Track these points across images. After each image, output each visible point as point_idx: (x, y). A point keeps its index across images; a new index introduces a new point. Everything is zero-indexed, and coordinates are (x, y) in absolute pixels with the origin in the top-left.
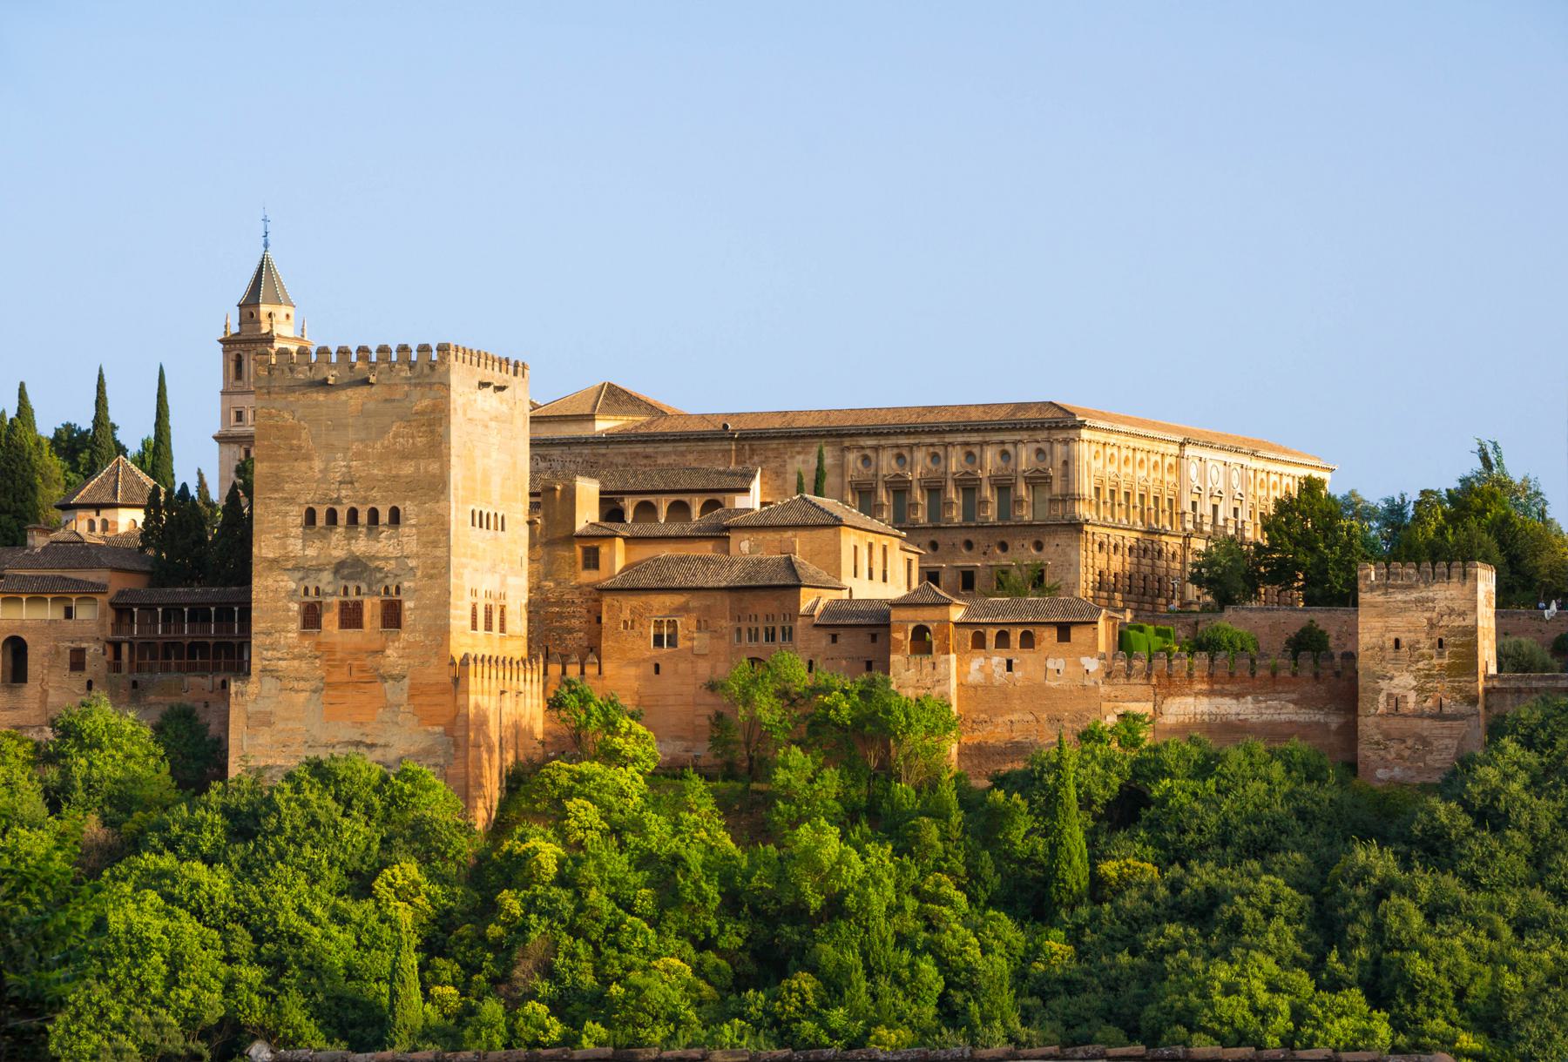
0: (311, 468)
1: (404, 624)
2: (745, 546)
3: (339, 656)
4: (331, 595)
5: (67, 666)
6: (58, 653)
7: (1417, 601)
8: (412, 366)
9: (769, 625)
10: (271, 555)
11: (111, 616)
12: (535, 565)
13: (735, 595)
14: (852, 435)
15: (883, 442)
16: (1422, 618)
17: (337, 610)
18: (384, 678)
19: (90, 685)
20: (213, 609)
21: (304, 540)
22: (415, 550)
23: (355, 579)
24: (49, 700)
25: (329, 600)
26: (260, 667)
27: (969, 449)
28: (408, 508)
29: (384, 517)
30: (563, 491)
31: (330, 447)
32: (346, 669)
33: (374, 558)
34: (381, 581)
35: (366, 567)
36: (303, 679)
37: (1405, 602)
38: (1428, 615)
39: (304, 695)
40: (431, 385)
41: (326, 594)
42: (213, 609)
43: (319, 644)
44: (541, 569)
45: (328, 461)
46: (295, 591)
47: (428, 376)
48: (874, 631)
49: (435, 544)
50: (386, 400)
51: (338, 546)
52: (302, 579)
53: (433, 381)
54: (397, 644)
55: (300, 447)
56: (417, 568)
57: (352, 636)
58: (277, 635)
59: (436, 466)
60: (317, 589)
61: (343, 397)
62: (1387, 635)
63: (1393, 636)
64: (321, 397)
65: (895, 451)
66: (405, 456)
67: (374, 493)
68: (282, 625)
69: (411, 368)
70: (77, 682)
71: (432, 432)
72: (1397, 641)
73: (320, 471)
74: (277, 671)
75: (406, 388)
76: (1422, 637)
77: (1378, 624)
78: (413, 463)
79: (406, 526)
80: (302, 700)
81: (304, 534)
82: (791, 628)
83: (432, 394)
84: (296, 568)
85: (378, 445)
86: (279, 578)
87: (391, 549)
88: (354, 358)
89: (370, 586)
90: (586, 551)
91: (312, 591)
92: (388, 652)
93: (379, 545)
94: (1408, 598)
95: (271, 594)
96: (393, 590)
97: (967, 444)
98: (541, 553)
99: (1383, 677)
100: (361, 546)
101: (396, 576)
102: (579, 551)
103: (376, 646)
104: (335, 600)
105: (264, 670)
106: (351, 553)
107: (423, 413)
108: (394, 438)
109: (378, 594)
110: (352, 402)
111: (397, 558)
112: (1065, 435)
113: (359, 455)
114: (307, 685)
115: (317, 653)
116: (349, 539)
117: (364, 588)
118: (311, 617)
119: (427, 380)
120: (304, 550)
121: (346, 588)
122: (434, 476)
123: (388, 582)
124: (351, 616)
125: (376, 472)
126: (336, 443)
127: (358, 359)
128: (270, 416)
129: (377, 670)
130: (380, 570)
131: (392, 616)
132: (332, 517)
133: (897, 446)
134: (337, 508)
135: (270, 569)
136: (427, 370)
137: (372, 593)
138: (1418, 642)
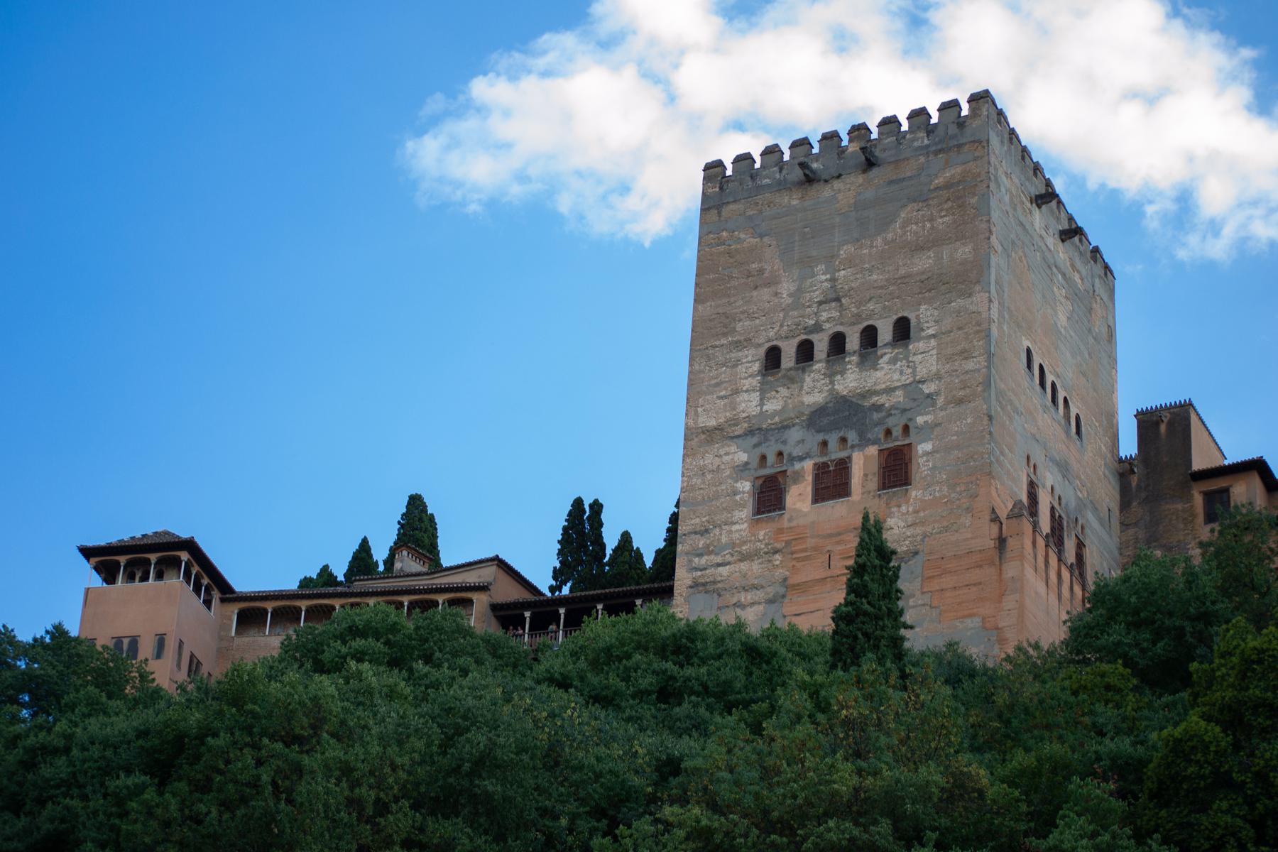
0: (776, 294)
3: (811, 542)
4: (801, 459)
10: (713, 423)
12: (1131, 531)
17: (809, 478)
21: (763, 392)
22: (934, 369)
23: (839, 429)
28: (925, 316)
29: (885, 333)
36: (755, 587)
41: (792, 459)
43: (780, 531)
46: (747, 463)
47: (953, 137)
50: (891, 182)
52: (755, 446)
54: (904, 508)
55: (761, 271)
56: (937, 393)
58: (717, 531)
60: (780, 454)
64: (793, 200)
66: (918, 248)
67: (871, 306)
68: (725, 515)
73: (790, 295)
74: (714, 582)
75: (922, 159)
79: (919, 340)
81: (762, 383)
85: (879, 241)
86: (722, 452)
87: (896, 376)
89: (861, 435)
90: (1209, 497)
91: (771, 459)
93: (879, 374)
95: (709, 477)
100: (851, 380)
101: (904, 411)
102: (1198, 500)
104: (808, 465)
105: (695, 585)
107: (948, 186)
108: (903, 227)
110: (840, 196)
111: (904, 386)
113: (850, 262)
114: (760, 595)
115: (778, 546)
116: (830, 376)
120: (761, 404)
121: (825, 444)
123: (890, 422)
125: (875, 277)
127: (850, 141)
130: (878, 408)
134: (814, 338)
135: (710, 441)
136: (953, 129)
137: (864, 442)
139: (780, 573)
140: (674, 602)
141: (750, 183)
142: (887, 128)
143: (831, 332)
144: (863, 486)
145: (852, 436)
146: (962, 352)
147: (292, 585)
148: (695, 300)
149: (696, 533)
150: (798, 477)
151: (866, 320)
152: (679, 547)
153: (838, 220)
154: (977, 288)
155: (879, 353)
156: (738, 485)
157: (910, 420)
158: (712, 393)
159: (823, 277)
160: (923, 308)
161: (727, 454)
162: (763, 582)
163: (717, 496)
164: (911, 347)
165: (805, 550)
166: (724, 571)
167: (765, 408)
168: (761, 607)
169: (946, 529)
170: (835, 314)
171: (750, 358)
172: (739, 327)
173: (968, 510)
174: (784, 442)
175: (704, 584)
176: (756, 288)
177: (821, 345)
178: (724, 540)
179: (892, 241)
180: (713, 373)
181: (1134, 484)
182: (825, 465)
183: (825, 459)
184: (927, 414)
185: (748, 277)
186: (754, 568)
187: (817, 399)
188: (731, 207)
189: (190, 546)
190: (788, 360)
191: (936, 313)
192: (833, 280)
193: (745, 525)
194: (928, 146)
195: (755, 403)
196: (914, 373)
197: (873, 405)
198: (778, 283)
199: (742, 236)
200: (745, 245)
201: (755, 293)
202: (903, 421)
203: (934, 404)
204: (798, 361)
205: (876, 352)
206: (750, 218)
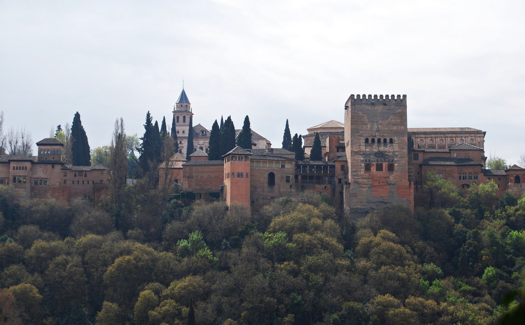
0: (367, 127)
1: (395, 170)
2: (455, 155)
3: (376, 178)
5: (285, 181)
6: (283, 177)
8: (396, 100)
9: (470, 175)
10: (356, 151)
14: (418, 134)
15: (427, 136)
18: (389, 184)
19: (291, 186)
20: (322, 167)
22: (397, 150)
24: (281, 190)
25: (373, 163)
27: (452, 138)
28: (395, 138)
29: (388, 141)
31: (373, 122)
33: (386, 152)
34: (388, 158)
39: (365, 189)
40: (401, 105)
41: (372, 161)
42: (322, 167)
43: (370, 175)
45: (372, 125)
50: (388, 109)
51: (375, 149)
52: (365, 157)
53: (402, 104)
54: (393, 175)
55: (364, 122)
56: (398, 155)
57: (380, 173)
59: (403, 127)
61: (376, 108)
65: (431, 138)
66: (394, 125)
70: (288, 186)
71: (402, 118)
74: (358, 182)
75: (394, 106)
78: (396, 127)
80: (365, 190)
81: (365, 144)
82: (477, 176)
84: (363, 154)
85: (386, 121)
87: (390, 150)
88: (379, 98)
89: (385, 160)
91: (368, 161)
92: (390, 177)
93: (387, 148)
95: (356, 161)
96: (391, 161)
97: (452, 137)
100: (382, 148)
101: (392, 157)
102: (413, 155)
104: (375, 163)
105: (355, 182)
106: (379, 150)
107: (399, 113)
111: (392, 152)
112: (479, 135)
113: (381, 124)
114: (367, 186)
115: (370, 177)
116: (378, 146)
118: (368, 168)
119: (400, 104)
120: (365, 149)
122: (402, 130)
125: (386, 128)
126: (374, 121)
128: (355, 113)
129: (387, 182)
131: (391, 168)
132: (373, 141)
133: (432, 137)
136: (400, 102)
137: (385, 161)
141: (360, 102)
142: (387, 97)
143: (378, 138)
144: (385, 170)
145: (383, 160)
146: (403, 148)
148: (351, 124)
149: (354, 172)
150: (373, 165)
151: (385, 137)
153: (378, 114)
155: (387, 144)
156: (362, 164)
157: (393, 159)
159: (376, 126)
160: (395, 137)
161: (359, 157)
162: (367, 184)
163: (358, 165)
165: (375, 179)
166: (360, 180)
167: (366, 150)
168: (367, 188)
169: (400, 181)
171: (363, 139)
174: (370, 158)
175: (356, 182)
176: (363, 125)
177: (376, 140)
179: (389, 122)
180: (356, 140)
184: (397, 158)
185: (361, 122)
186: (366, 181)
187: (375, 151)
188: (357, 106)
190: (370, 141)
191: (398, 139)
192: (378, 127)
193: (363, 172)
194: (395, 104)
195: (364, 148)
197: (386, 154)
198: (367, 125)
200: (360, 115)
201: (363, 126)
202: (392, 159)
203: (398, 157)
205: (386, 144)
206: (361, 109)
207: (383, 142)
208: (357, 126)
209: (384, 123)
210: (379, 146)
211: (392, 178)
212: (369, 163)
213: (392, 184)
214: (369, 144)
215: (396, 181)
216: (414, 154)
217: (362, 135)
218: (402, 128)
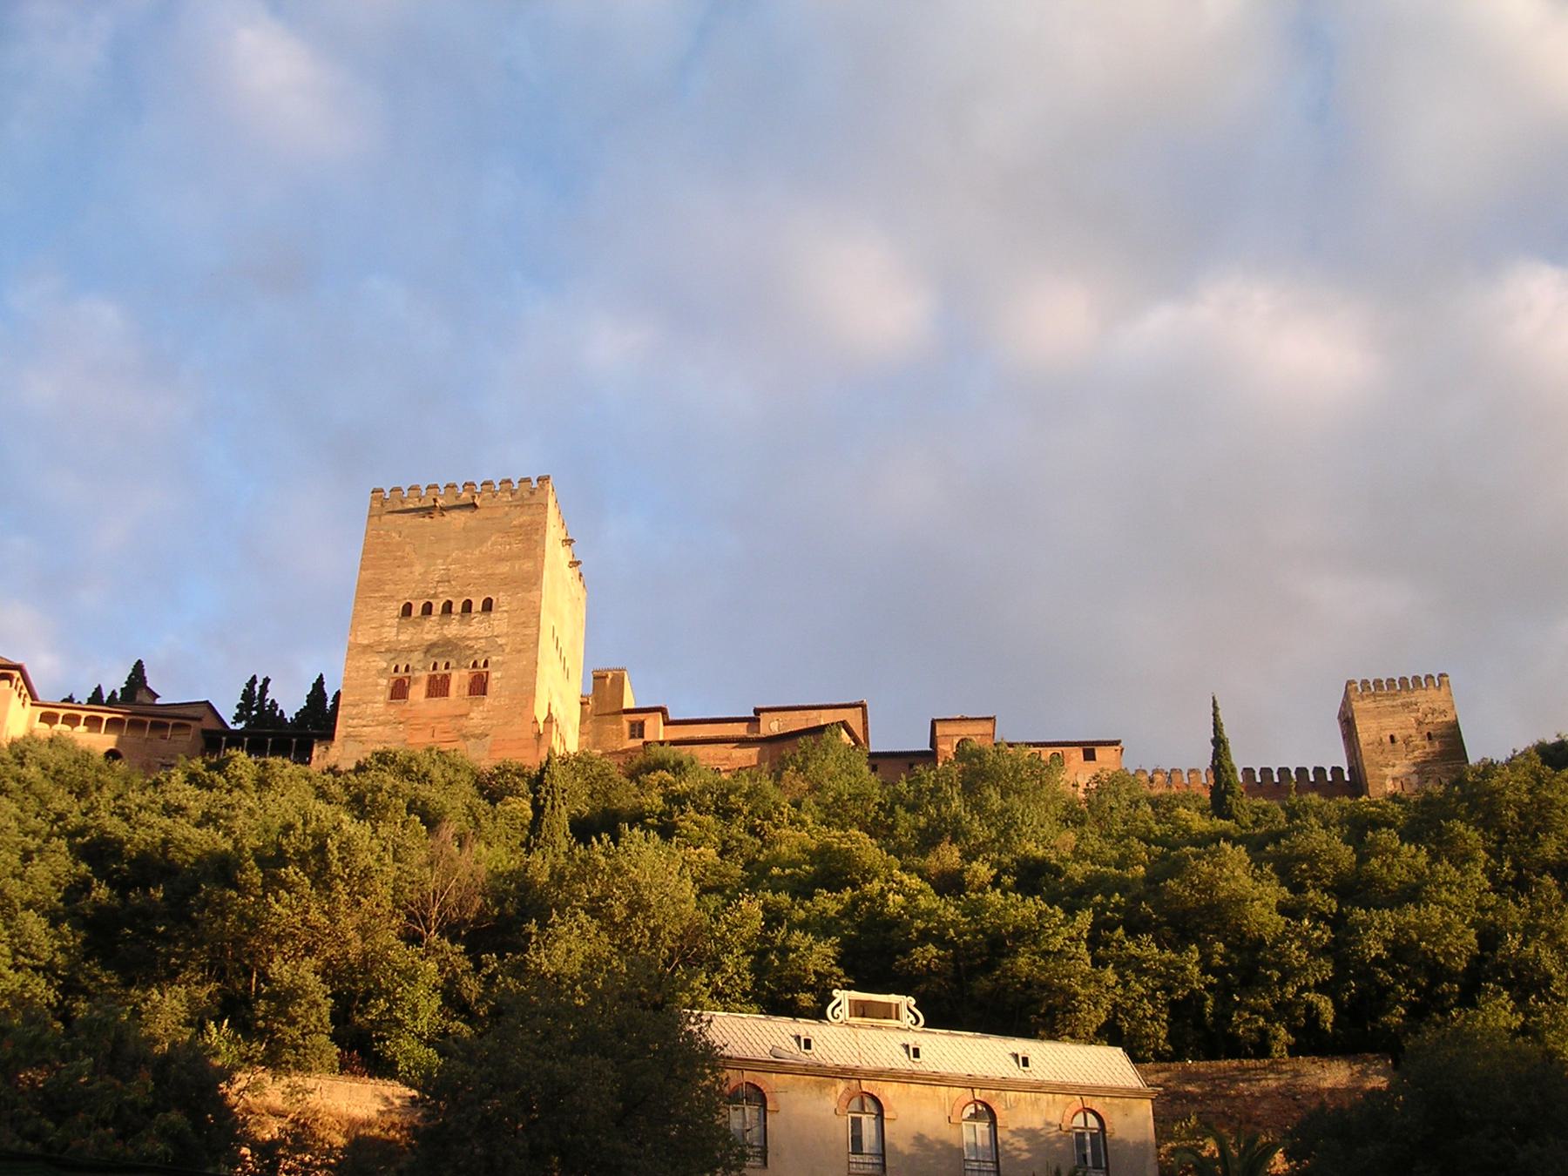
7: (1403, 705)
10: (366, 642)
11: (201, 744)
12: (585, 737)
13: (774, 746)
16: (1410, 719)
18: (465, 737)
22: (505, 630)
25: (417, 674)
26: (344, 734)
28: (500, 599)
29: (477, 605)
30: (612, 679)
32: (429, 731)
35: (456, 645)
37: (1393, 706)
38: (1414, 715)
41: (414, 670)
43: (404, 711)
44: (590, 741)
48: (912, 760)
49: (525, 625)
51: (431, 630)
54: (481, 708)
57: (439, 704)
60: (407, 667)
62: (1383, 733)
63: (1389, 733)
66: (501, 559)
68: (370, 697)
69: (512, 495)
72: (1392, 737)
74: (360, 736)
75: (507, 509)
76: (1413, 732)
77: (1373, 725)
78: (508, 564)
79: (497, 612)
81: (399, 623)
83: (530, 512)
84: (388, 651)
85: (477, 552)
88: (461, 491)
90: (632, 724)
91: (402, 668)
92: (472, 715)
94: (1394, 703)
95: (362, 673)
96: (481, 664)
98: (591, 727)
99: (1387, 765)
100: (453, 629)
101: (485, 652)
102: (626, 726)
103: (463, 711)
104: (423, 675)
105: (348, 736)
107: (521, 526)
108: (492, 545)
109: (467, 667)
111: (486, 638)
113: (455, 562)
115: (402, 719)
117: (453, 663)
118: (399, 691)
120: (398, 635)
121: (435, 664)
122: (528, 572)
123: (476, 657)
124: (438, 687)
125: (473, 572)
128: (379, 536)
131: (479, 686)
132: (427, 609)
136: (526, 495)
138: (1411, 736)
139: (401, 736)
140: (334, 744)
143: (444, 601)
146: (524, 623)
147: (57, 700)
150: (417, 681)
151: (468, 595)
152: (340, 713)
154: (535, 587)
155: (472, 616)
158: (367, 624)
160: (501, 594)
164: (492, 615)
170: (446, 589)
172: (387, 587)
173: (520, 714)
177: (438, 607)
178: (368, 712)
179: (486, 553)
181: (589, 710)
182: (435, 676)
183: (434, 673)
189: (19, 668)
190: (417, 610)
196: (493, 631)
199: (393, 535)
203: (503, 651)
204: (423, 614)
207: (460, 611)
208: (379, 571)
209: (468, 556)
210: (445, 624)
211: (479, 715)
212: (407, 674)
213: (474, 736)
214: (411, 619)
215: (493, 726)
216: (630, 722)
217: (393, 597)
218: (525, 566)
